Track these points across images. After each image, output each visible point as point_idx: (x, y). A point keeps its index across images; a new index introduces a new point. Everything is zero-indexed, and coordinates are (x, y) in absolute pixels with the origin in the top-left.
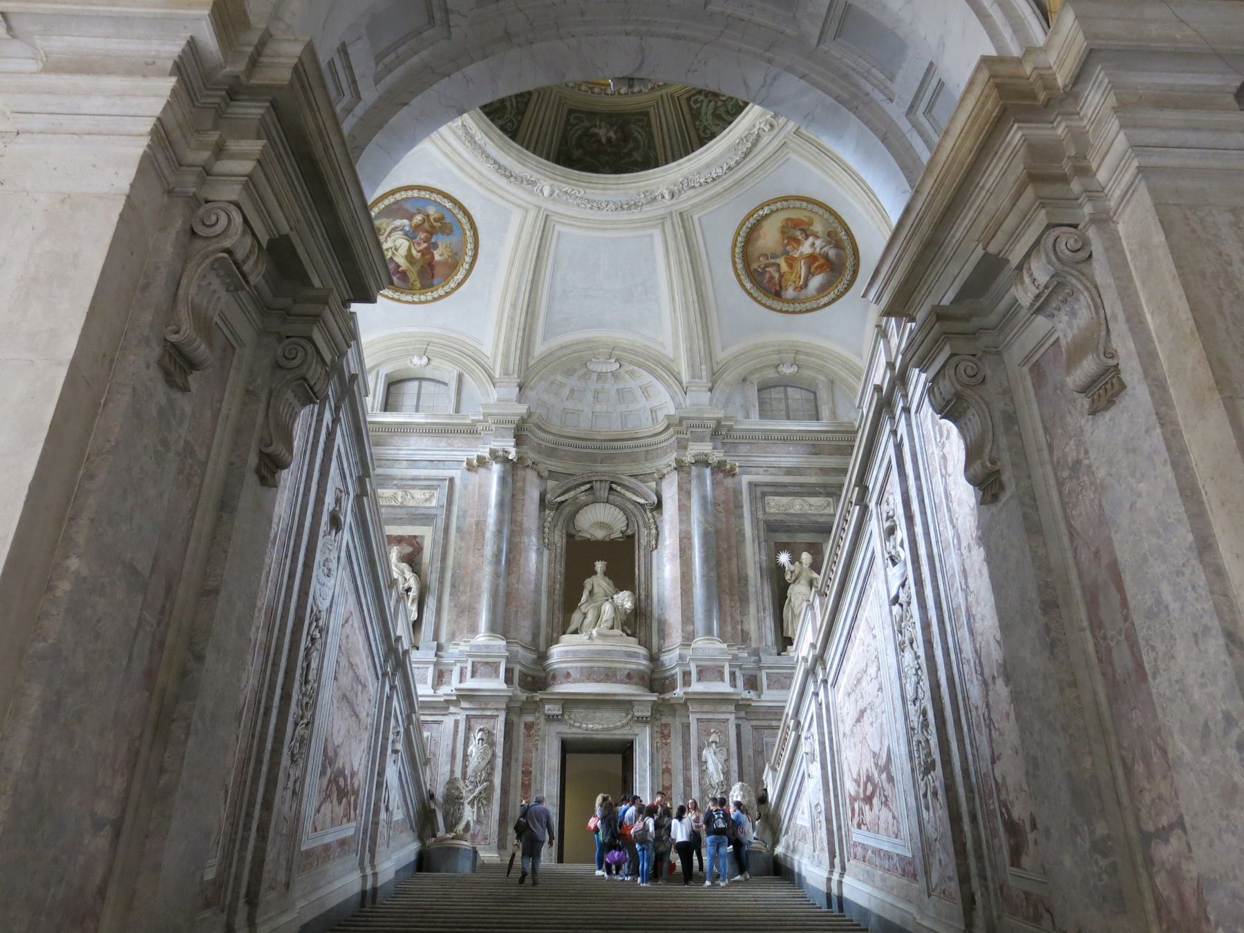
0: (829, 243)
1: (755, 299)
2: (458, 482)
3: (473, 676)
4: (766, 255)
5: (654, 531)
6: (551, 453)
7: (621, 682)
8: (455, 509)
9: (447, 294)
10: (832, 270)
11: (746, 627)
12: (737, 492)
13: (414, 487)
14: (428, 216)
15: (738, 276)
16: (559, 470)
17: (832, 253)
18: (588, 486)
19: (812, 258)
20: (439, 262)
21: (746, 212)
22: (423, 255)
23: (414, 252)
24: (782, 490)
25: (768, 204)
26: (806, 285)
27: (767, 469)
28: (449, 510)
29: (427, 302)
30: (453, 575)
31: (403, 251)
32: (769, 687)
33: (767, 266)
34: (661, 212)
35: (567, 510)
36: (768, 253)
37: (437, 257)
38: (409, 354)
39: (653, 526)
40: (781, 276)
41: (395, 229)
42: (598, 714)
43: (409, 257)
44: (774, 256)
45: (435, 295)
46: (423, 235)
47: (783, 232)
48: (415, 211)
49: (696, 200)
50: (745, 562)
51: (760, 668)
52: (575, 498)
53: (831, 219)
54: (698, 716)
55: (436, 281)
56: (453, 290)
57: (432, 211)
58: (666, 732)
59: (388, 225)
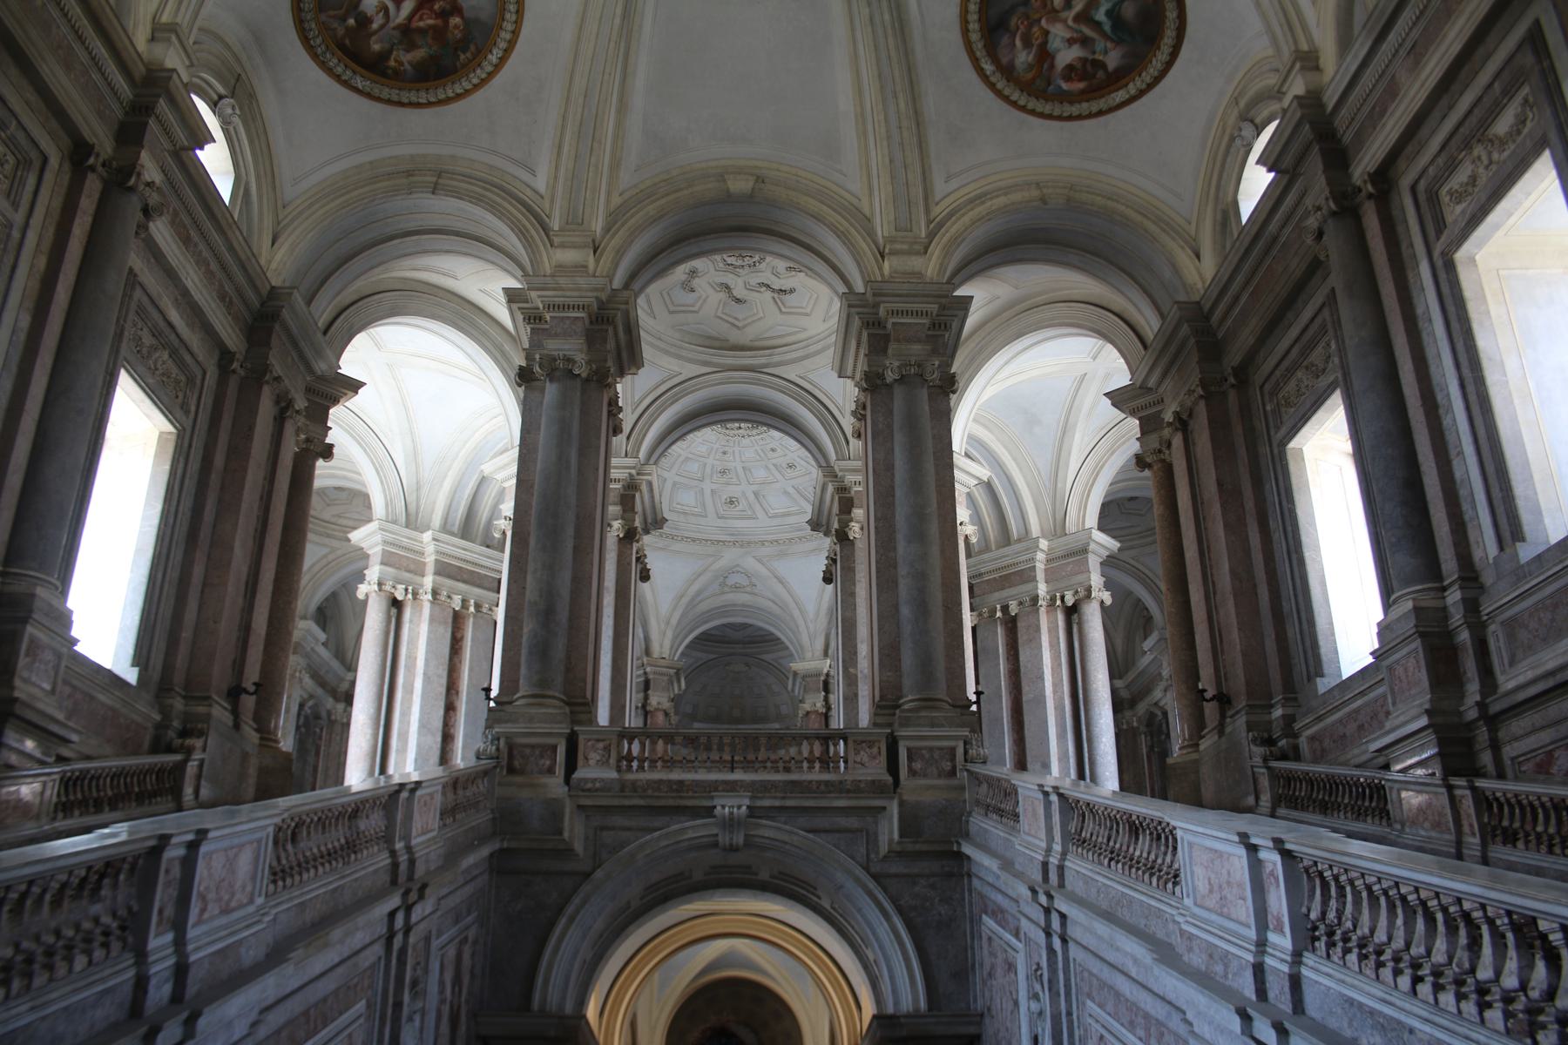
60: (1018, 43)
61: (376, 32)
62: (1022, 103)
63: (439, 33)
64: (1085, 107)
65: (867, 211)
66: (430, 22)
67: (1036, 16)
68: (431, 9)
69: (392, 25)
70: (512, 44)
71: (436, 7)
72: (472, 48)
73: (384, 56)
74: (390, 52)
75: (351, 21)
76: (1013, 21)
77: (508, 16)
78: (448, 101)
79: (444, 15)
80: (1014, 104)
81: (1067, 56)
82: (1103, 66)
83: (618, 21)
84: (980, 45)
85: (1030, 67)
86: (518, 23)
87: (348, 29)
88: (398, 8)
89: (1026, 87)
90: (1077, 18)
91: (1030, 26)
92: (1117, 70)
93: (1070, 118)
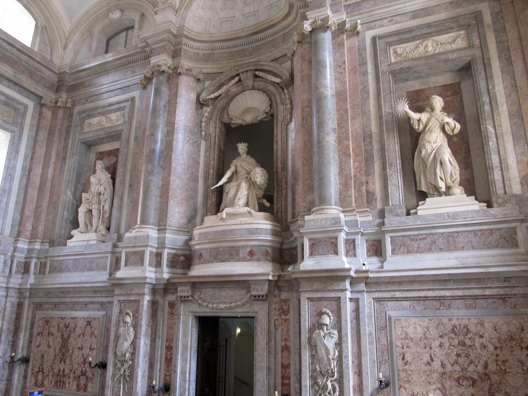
2: (137, 100)
3: (126, 265)
5: (289, 106)
6: (207, 58)
7: (244, 260)
8: (134, 122)
11: (371, 187)
12: (362, 49)
13: (110, 112)
16: (214, 71)
18: (237, 79)
24: (408, 36)
27: (391, 19)
28: (130, 124)
30: (131, 177)
32: (393, 252)
35: (221, 103)
38: (110, 11)
39: (288, 102)
42: (224, 293)
50: (369, 120)
51: (384, 232)
52: (227, 92)
54: (308, 295)
58: (285, 307)
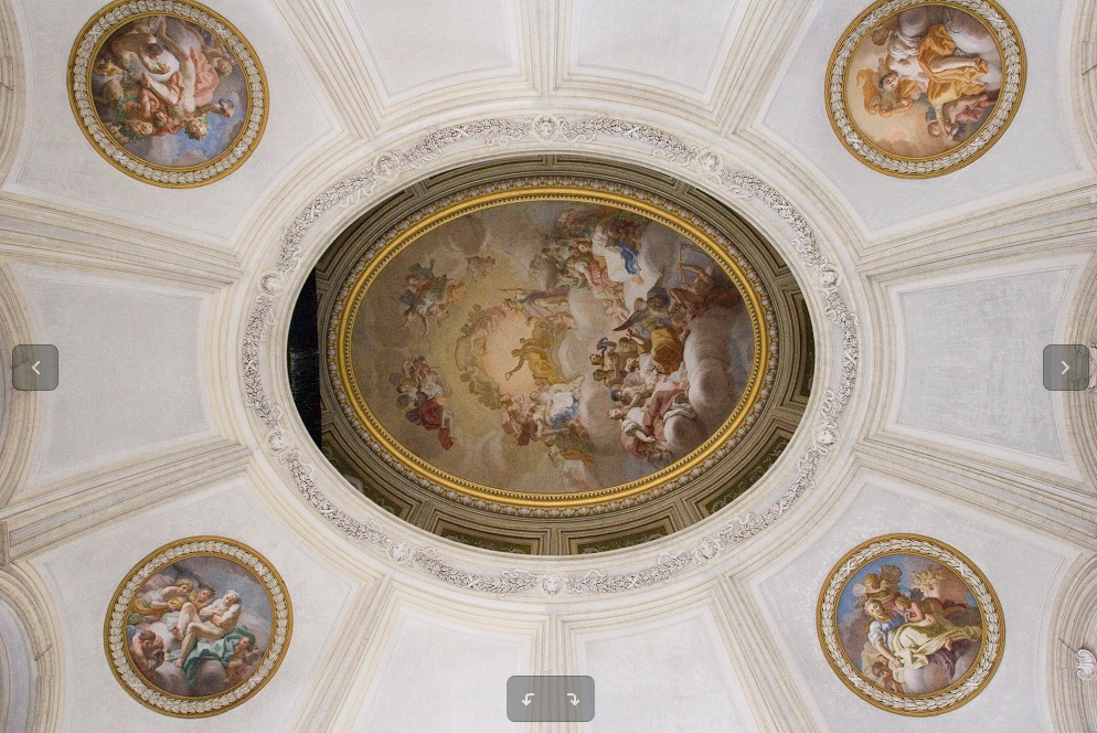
0: (894, 38)
1: (1002, 129)
4: (930, 127)
9: (989, 590)
10: (942, 22)
14: (869, 595)
15: (963, 163)
17: (911, 30)
19: (926, 58)
20: (940, 591)
21: (861, 167)
22: (930, 613)
23: (922, 624)
25: (842, 138)
26: (974, 56)
29: (1001, 622)
31: (921, 639)
33: (947, 122)
34: (857, 284)
36: (925, 124)
37: (935, 594)
38: (1074, 673)
40: (963, 97)
41: (883, 643)
43: (932, 631)
44: (931, 114)
45: (989, 608)
46: (899, 607)
47: (890, 109)
48: (861, 609)
49: (838, 242)
53: (849, 45)
55: (970, 603)
56: (983, 580)
57: (860, 589)
59: (874, 650)
60: (167, 589)
61: (141, 59)
62: (118, 607)
63: (138, 112)
64: (121, 660)
65: (11, 501)
66: (148, 108)
67: (192, 598)
68: (160, 109)
69: (147, 74)
70: (132, 173)
71: (162, 114)
72: (126, 139)
73: (118, 60)
74: (123, 68)
75: (153, 40)
76: (185, 581)
77: (158, 173)
78: (77, 110)
79: (154, 120)
80: (115, 601)
81: (162, 631)
82: (159, 663)
83: (163, 265)
84: (164, 560)
85: (148, 605)
86: (151, 181)
87: (147, 36)
88: (162, 82)
89: (131, 607)
90: (195, 629)
91: (183, 595)
92: (159, 675)
93: (109, 652)
